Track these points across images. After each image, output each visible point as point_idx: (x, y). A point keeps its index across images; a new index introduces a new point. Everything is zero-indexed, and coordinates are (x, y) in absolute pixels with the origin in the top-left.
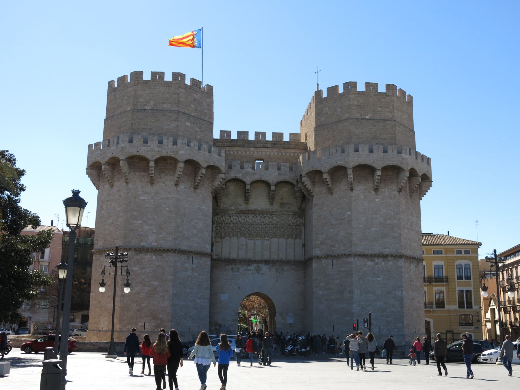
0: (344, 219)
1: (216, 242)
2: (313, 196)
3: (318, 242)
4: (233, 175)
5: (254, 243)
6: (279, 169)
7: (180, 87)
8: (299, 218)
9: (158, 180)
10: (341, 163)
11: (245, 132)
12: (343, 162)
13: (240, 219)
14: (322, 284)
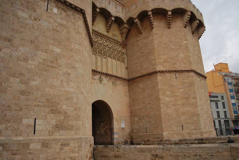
0: (181, 46)
2: (153, 28)
3: (162, 61)
5: (96, 58)
6: (117, 8)
8: (123, 48)
10: (183, 7)
12: (184, 6)
14: (168, 93)
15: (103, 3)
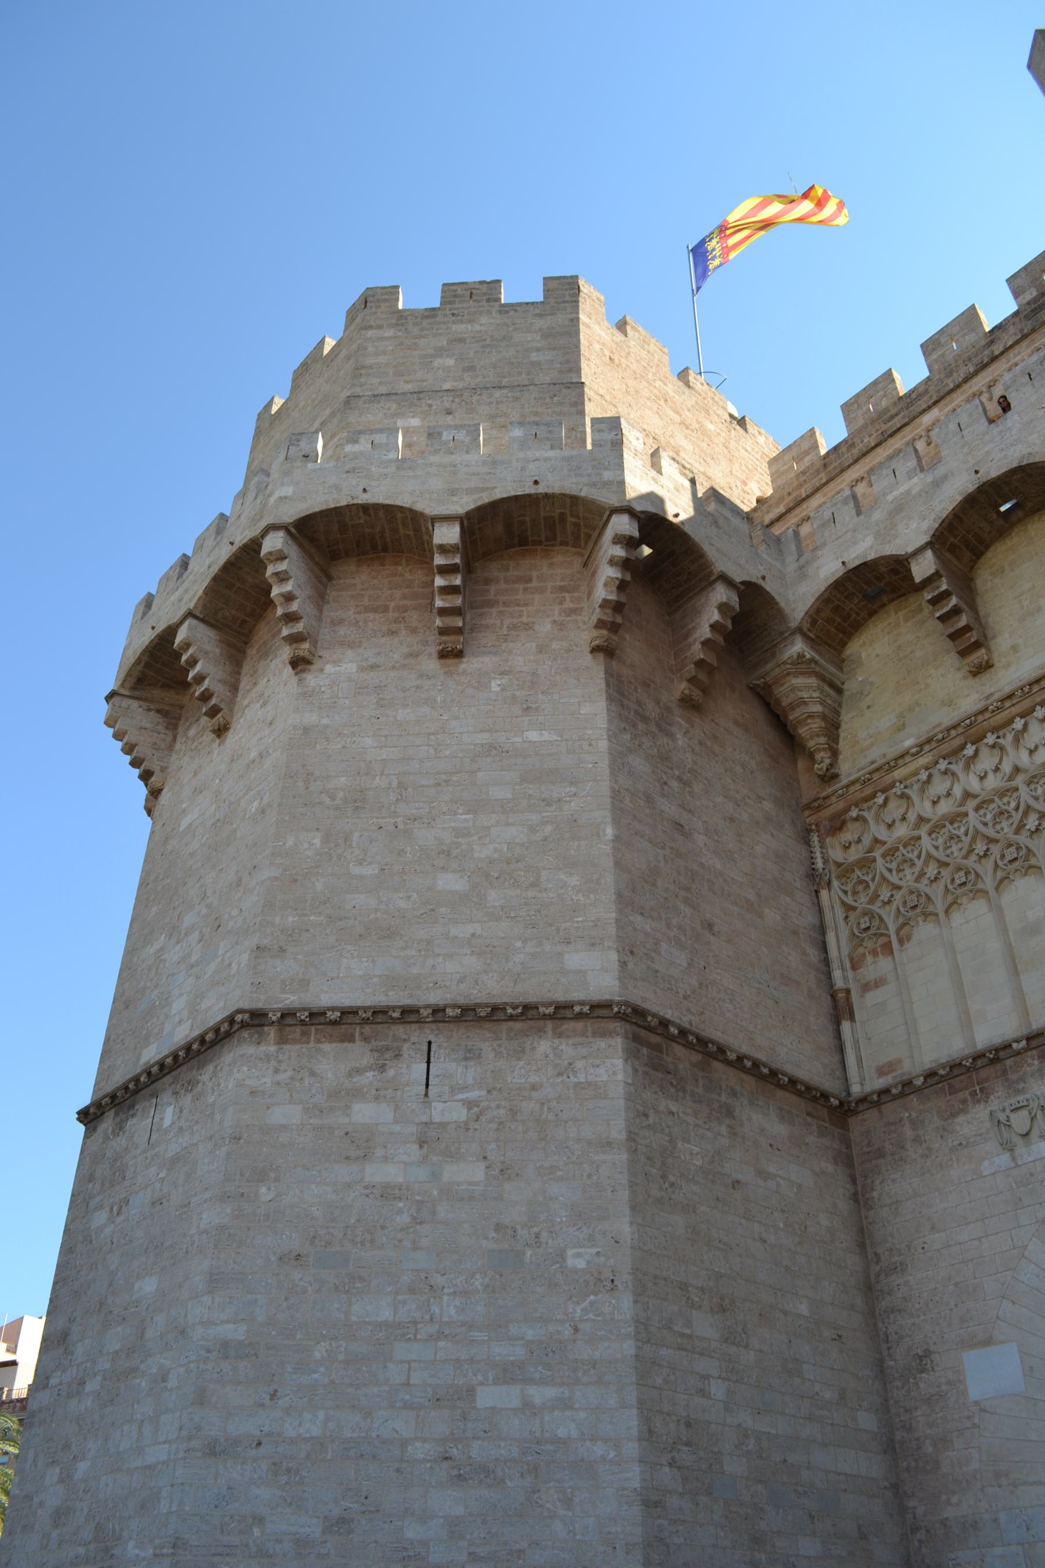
1: (866, 988)
4: (828, 569)
7: (371, 327)
9: (246, 702)
11: (875, 383)
13: (973, 784)
15: (945, 478)
